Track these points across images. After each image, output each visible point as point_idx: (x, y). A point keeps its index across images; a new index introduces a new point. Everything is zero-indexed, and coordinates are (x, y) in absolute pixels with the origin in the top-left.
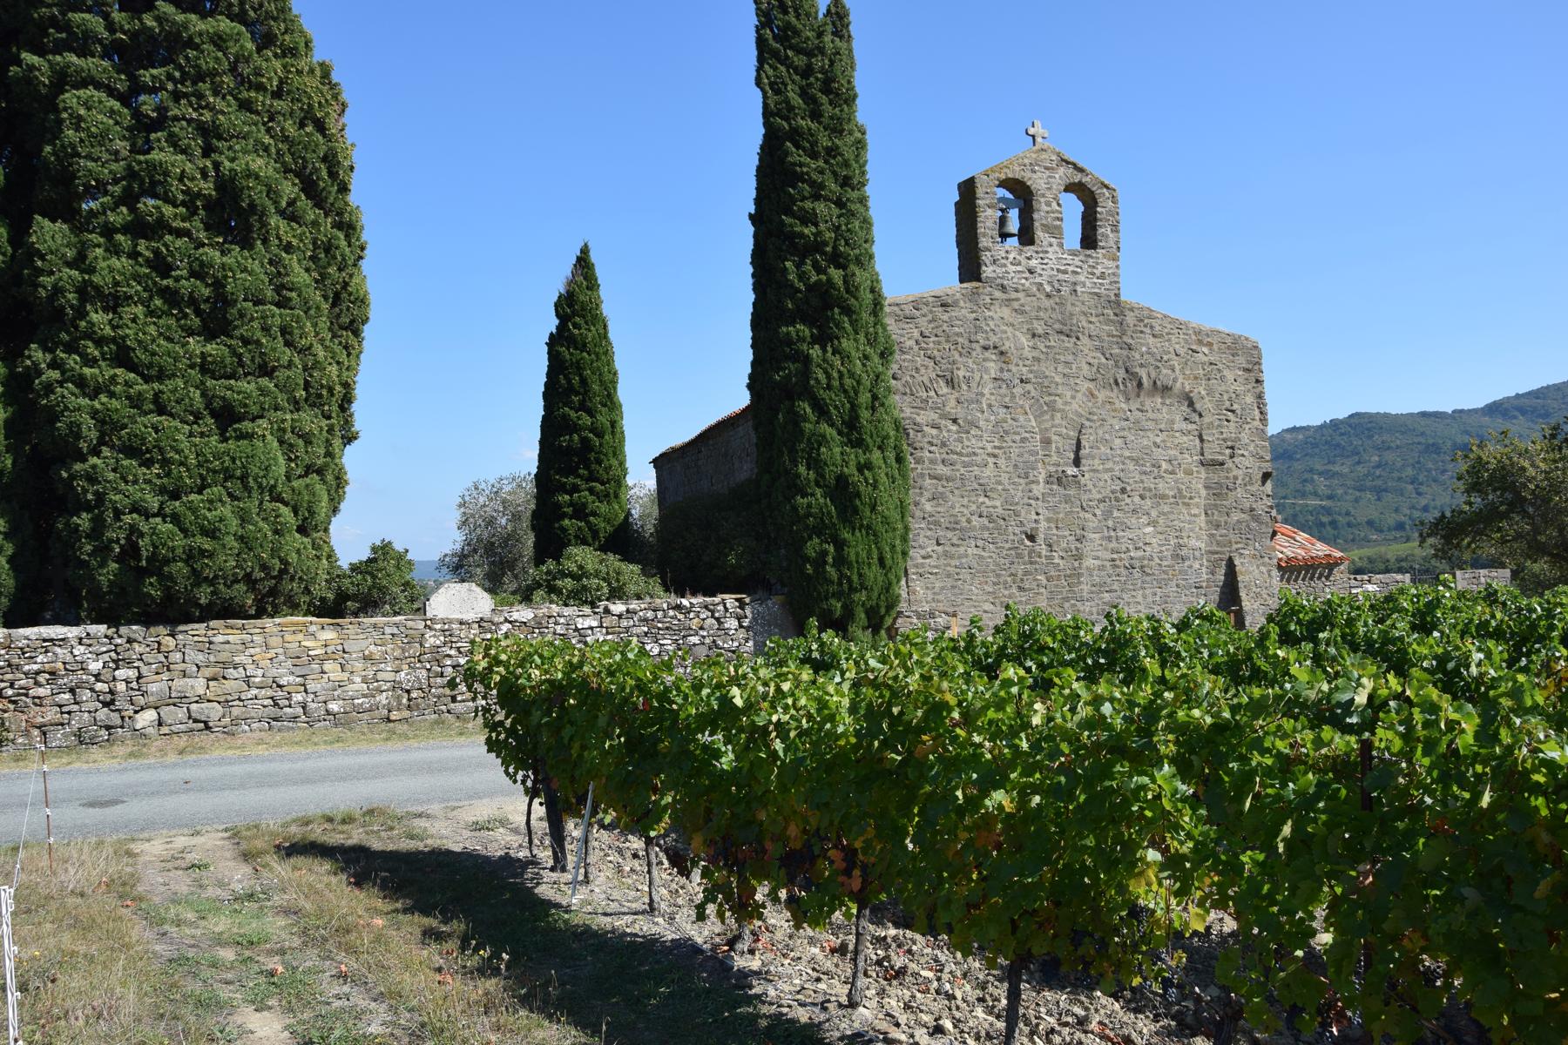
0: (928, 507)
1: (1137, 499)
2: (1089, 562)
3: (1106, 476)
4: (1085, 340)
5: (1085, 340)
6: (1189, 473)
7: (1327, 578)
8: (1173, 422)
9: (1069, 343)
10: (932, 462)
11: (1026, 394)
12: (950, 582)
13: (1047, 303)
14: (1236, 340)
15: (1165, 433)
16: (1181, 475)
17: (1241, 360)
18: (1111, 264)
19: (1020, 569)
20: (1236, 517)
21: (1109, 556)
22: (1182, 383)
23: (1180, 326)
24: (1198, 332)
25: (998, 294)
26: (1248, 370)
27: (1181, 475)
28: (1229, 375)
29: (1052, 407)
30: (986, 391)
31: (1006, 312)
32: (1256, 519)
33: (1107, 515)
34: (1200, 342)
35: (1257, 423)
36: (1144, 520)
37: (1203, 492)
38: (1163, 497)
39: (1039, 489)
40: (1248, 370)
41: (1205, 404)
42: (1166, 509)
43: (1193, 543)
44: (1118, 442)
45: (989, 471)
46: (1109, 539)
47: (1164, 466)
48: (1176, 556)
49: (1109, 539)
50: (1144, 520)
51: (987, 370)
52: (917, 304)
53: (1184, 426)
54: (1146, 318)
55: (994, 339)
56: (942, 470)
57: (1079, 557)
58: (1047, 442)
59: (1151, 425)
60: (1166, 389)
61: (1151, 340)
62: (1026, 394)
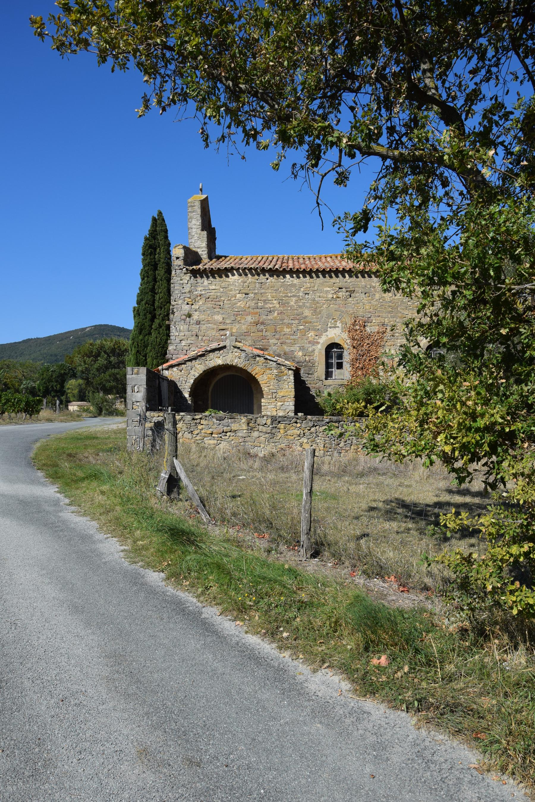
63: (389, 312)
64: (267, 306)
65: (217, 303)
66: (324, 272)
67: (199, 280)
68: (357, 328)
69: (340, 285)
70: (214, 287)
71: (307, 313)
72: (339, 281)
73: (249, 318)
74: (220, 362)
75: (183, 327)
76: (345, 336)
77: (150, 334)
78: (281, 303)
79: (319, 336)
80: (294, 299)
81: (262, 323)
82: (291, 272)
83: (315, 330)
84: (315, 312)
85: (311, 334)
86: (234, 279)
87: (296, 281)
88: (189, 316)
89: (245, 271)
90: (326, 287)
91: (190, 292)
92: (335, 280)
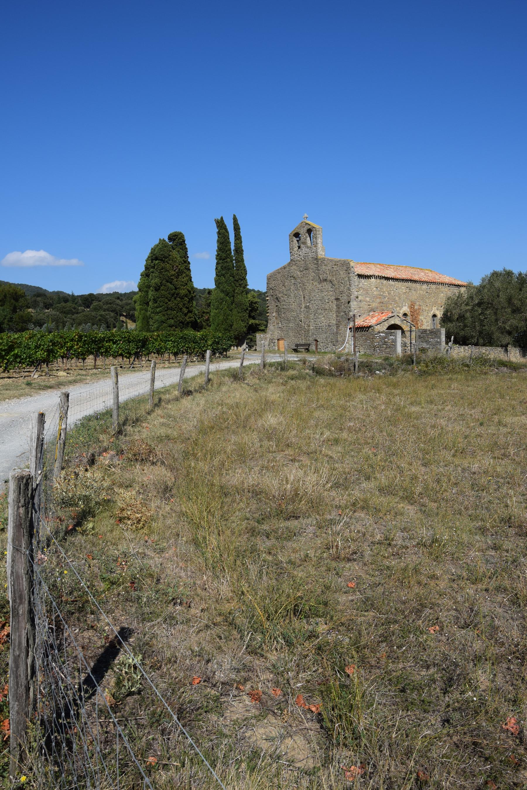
0: (283, 315)
1: (321, 311)
2: (312, 328)
3: (315, 305)
4: (311, 270)
5: (311, 270)
6: (332, 302)
7: (367, 331)
8: (328, 288)
9: (307, 271)
10: (283, 305)
11: (300, 287)
12: (287, 332)
13: (303, 262)
14: (344, 261)
15: (328, 293)
16: (330, 303)
17: (345, 268)
18: (315, 248)
19: (299, 329)
20: (342, 314)
21: (315, 326)
22: (329, 278)
23: (331, 261)
24: (335, 262)
25: (294, 263)
26: (346, 270)
27: (330, 303)
28: (341, 273)
29: (305, 288)
30: (292, 287)
31: (294, 267)
32: (346, 314)
33: (315, 315)
34: (335, 265)
35: (348, 286)
36: (322, 316)
37: (335, 307)
38: (326, 309)
39: (302, 310)
40: (346, 270)
41: (335, 282)
42: (327, 312)
43: (332, 322)
44: (317, 296)
45: (293, 306)
46: (315, 321)
47: (327, 301)
48: (329, 326)
49: (315, 321)
50: (322, 316)
51: (291, 282)
52: (281, 269)
53: (332, 289)
54: (324, 259)
55: (292, 274)
56: (285, 307)
57: (309, 326)
58: (304, 297)
59: (324, 290)
60: (326, 280)
61: (324, 267)
62: (300, 287)
63: (422, 300)
64: (384, 294)
65: (367, 292)
66: (403, 280)
67: (361, 279)
68: (412, 306)
69: (407, 286)
70: (366, 284)
71: (397, 298)
72: (406, 284)
73: (378, 300)
74: (393, 323)
75: (355, 303)
76: (409, 310)
77: (233, 296)
78: (389, 294)
79: (401, 309)
80: (393, 292)
81: (382, 303)
82: (392, 279)
83: (400, 307)
84: (400, 298)
85: (398, 309)
86: (373, 280)
87: (393, 283)
88: (357, 297)
89: (376, 277)
90: (402, 287)
91: (358, 285)
92: (405, 284)
